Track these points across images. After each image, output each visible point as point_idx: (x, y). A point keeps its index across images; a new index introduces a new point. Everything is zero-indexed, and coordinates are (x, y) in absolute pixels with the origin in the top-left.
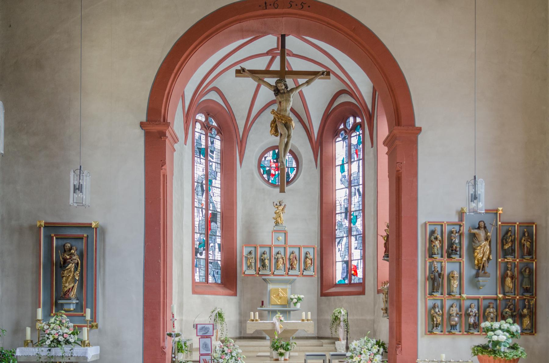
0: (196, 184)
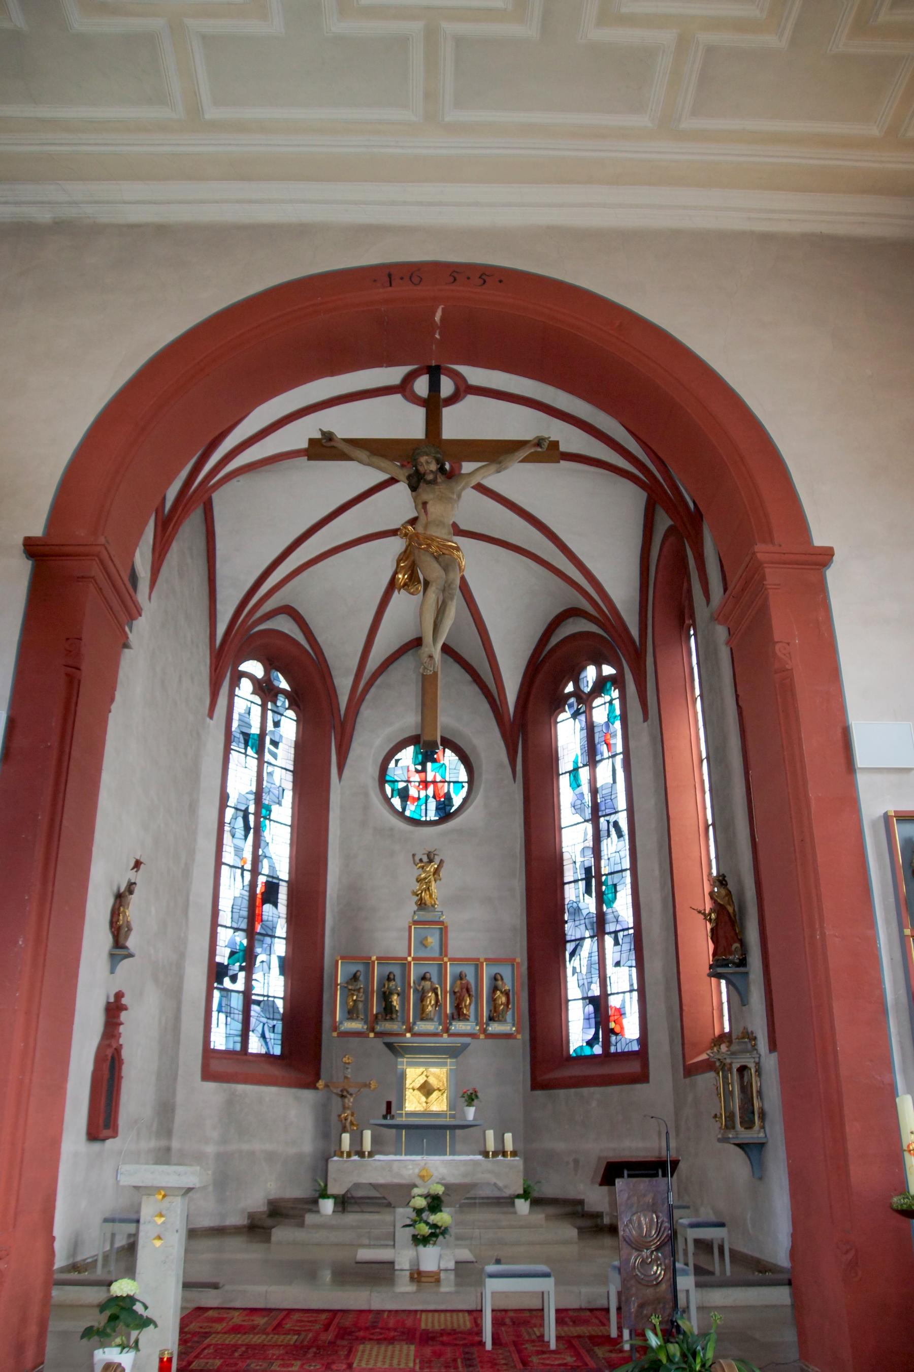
0: (229, 813)
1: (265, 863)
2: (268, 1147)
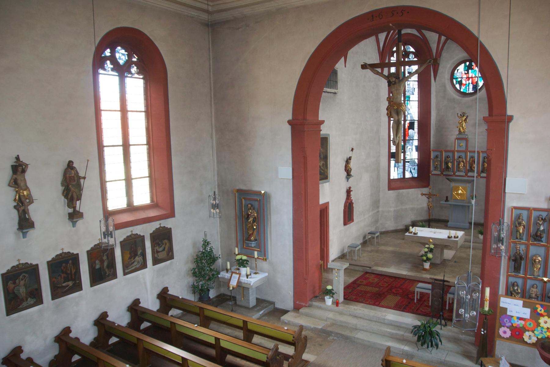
1: (409, 116)
2: (411, 206)
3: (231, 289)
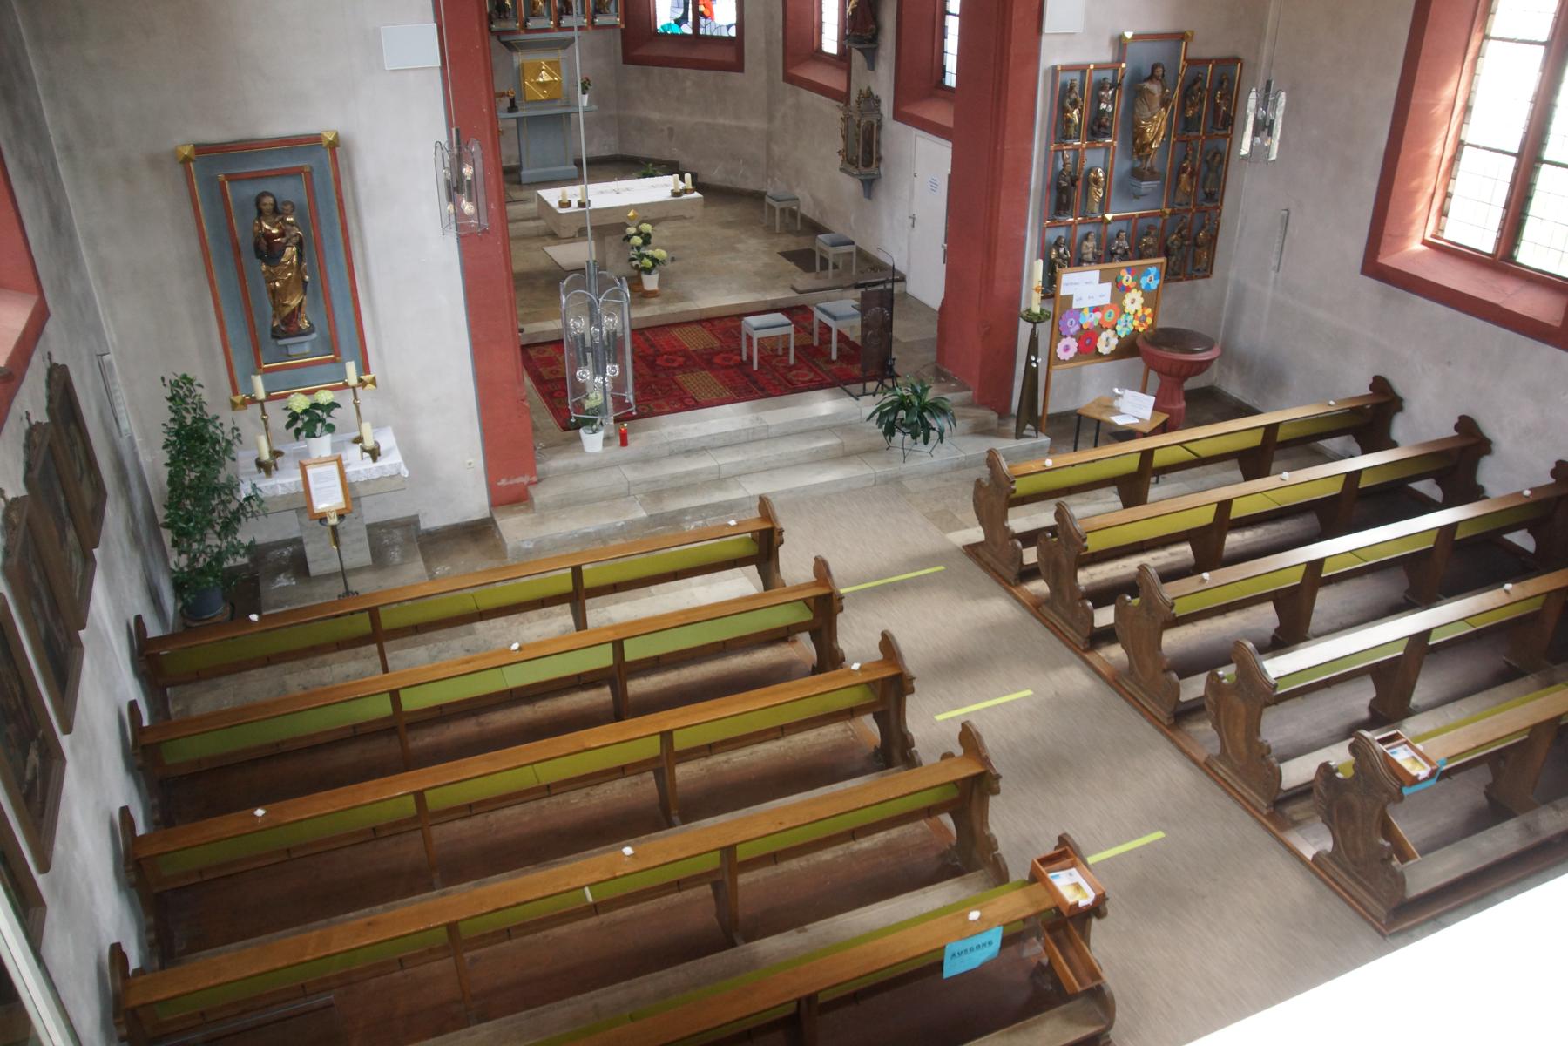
3: (333, 521)
